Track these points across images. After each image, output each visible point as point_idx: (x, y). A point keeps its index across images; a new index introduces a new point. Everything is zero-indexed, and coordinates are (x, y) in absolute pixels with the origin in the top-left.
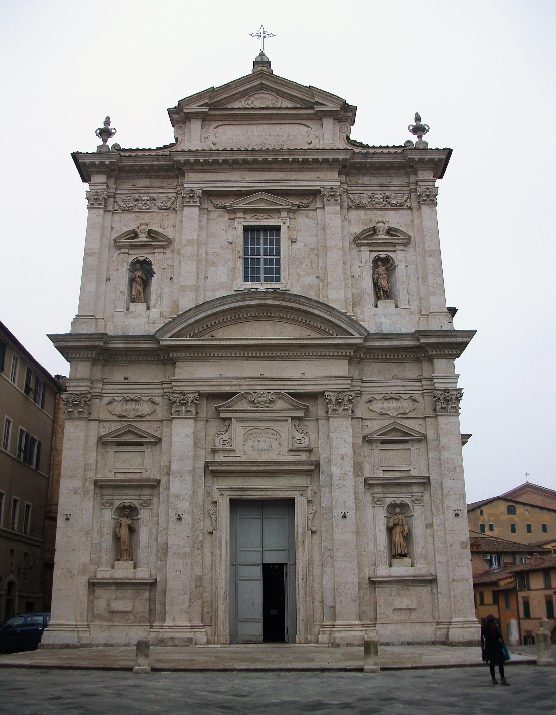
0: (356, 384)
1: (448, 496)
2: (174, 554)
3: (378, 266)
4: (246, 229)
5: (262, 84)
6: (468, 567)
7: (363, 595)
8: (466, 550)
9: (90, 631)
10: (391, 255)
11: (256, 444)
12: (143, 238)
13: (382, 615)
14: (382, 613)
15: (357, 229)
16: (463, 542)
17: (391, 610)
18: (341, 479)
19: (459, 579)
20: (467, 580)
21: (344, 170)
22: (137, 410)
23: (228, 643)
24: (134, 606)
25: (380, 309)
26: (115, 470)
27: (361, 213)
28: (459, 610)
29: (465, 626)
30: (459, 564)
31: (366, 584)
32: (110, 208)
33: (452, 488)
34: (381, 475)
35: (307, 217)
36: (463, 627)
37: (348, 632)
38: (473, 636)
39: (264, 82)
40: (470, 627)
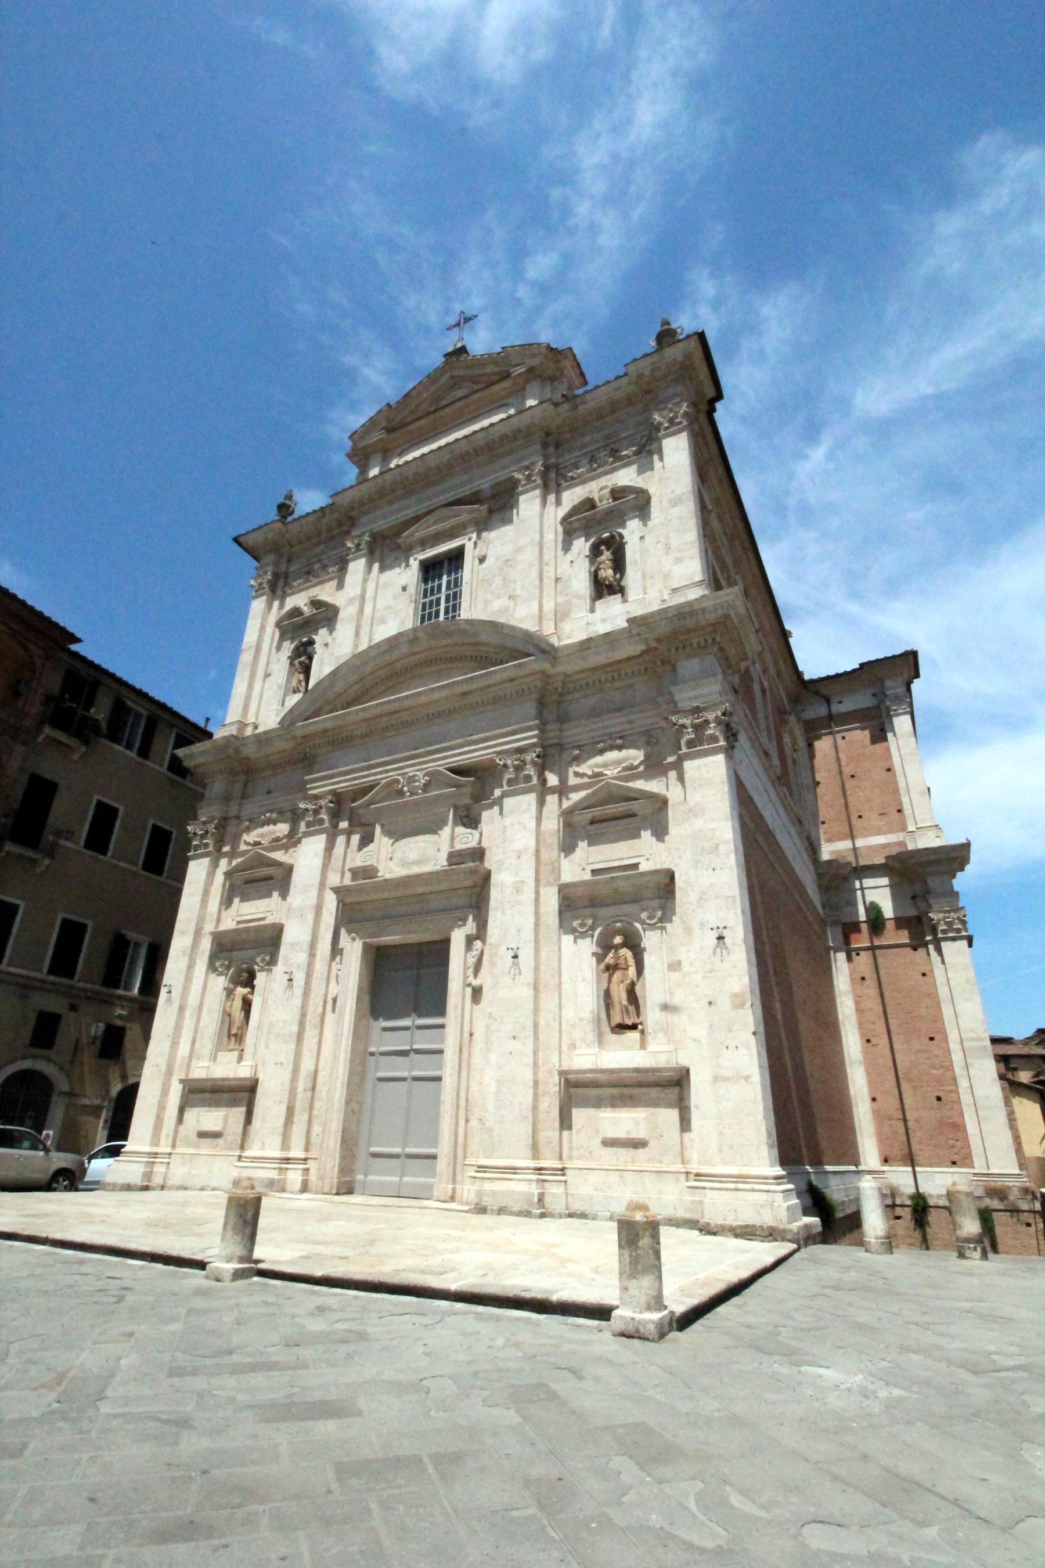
0: (551, 735)
1: (703, 901)
2: (278, 1036)
3: (601, 553)
5: (452, 377)
6: (747, 1048)
7: (549, 1106)
8: (741, 1011)
9: (168, 1163)
11: (406, 854)
13: (582, 1152)
14: (582, 1147)
16: (735, 995)
17: (599, 1141)
18: (515, 892)
19: (730, 1075)
20: (747, 1078)
21: (551, 438)
22: (274, 832)
23: (334, 1191)
24: (226, 1122)
25: (598, 614)
26: (239, 919)
28: (731, 1147)
29: (740, 1186)
30: (728, 1042)
31: (555, 1085)
33: (711, 885)
34: (587, 876)
36: (737, 1190)
37: (505, 1182)
38: (759, 1213)
39: (455, 373)
40: (753, 1190)
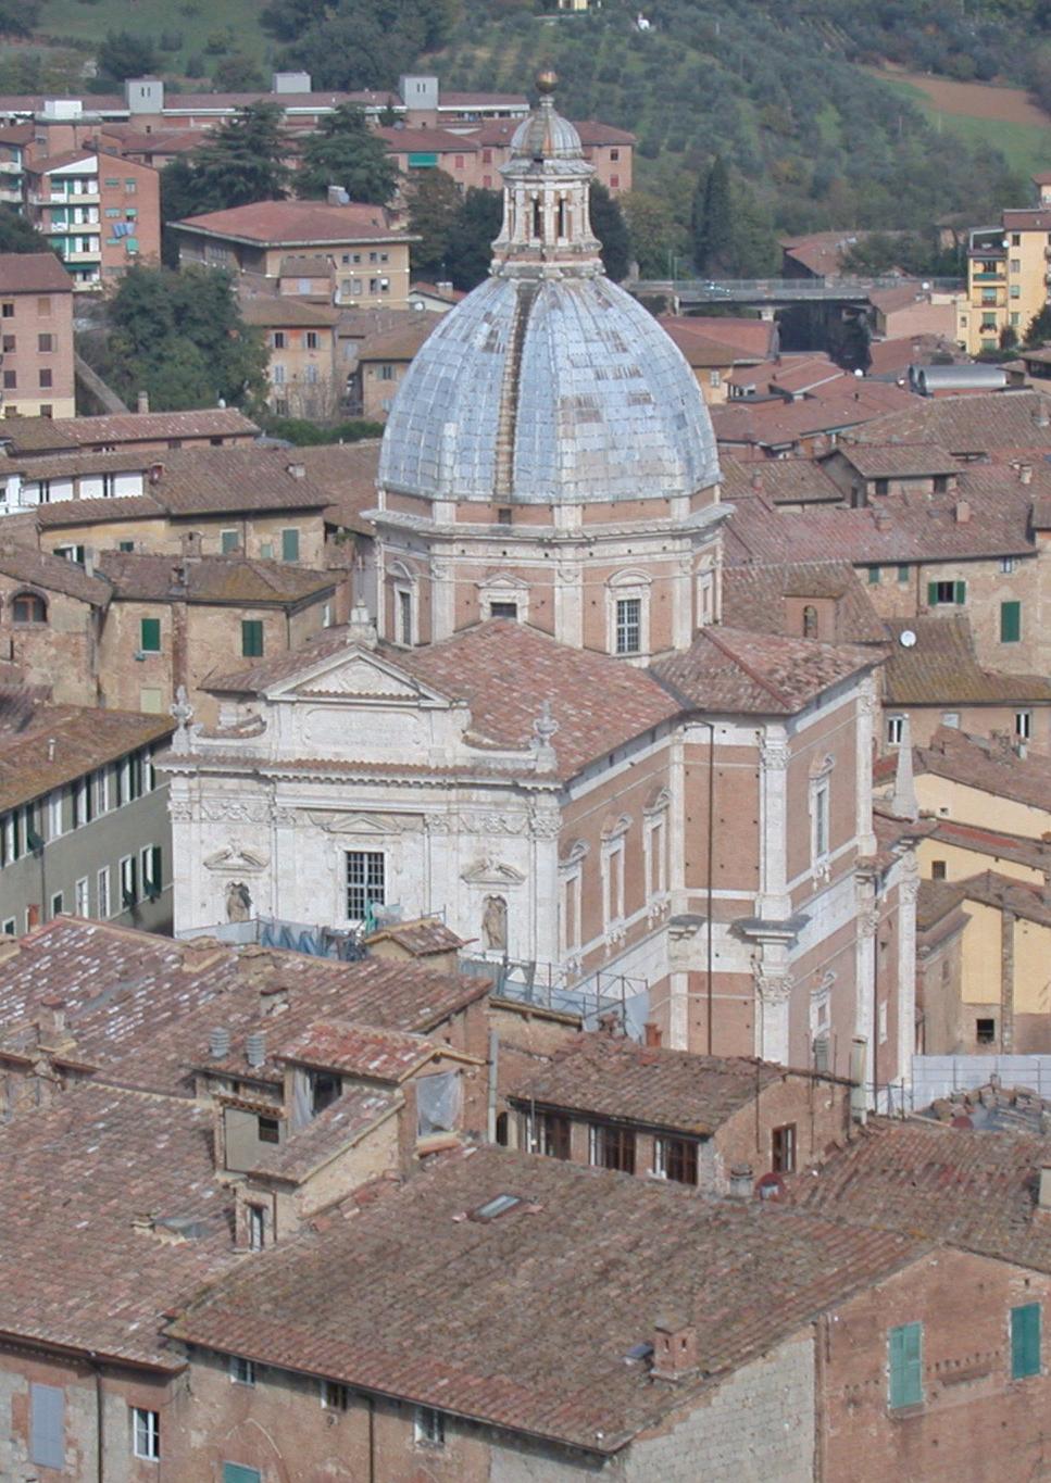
4: (349, 854)
10: (504, 895)
12: (236, 861)
15: (467, 860)
27: (474, 838)
32: (196, 817)
35: (415, 841)
